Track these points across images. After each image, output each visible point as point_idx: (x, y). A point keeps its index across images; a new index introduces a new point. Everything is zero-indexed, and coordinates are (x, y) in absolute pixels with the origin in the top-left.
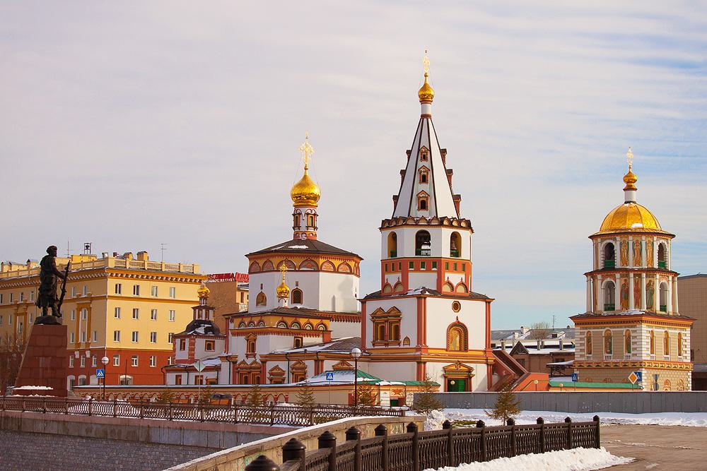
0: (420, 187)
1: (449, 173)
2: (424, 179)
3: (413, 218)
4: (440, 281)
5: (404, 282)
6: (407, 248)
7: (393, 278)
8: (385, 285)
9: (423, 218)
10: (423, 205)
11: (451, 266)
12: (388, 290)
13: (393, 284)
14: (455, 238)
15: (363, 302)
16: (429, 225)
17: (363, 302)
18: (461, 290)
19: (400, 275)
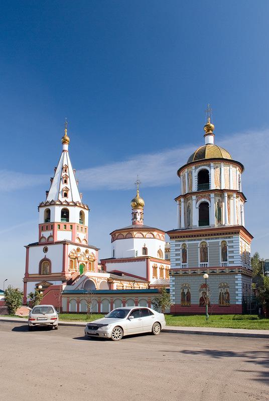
0: (63, 186)
1: (77, 182)
2: (66, 182)
3: (60, 201)
4: (73, 237)
5: (52, 236)
6: (57, 216)
7: (46, 234)
8: (41, 238)
9: (66, 201)
10: (66, 195)
11: (80, 228)
12: (43, 241)
13: (47, 238)
14: (81, 214)
15: (28, 247)
16: (68, 204)
17: (28, 247)
18: (84, 243)
19: (52, 232)
